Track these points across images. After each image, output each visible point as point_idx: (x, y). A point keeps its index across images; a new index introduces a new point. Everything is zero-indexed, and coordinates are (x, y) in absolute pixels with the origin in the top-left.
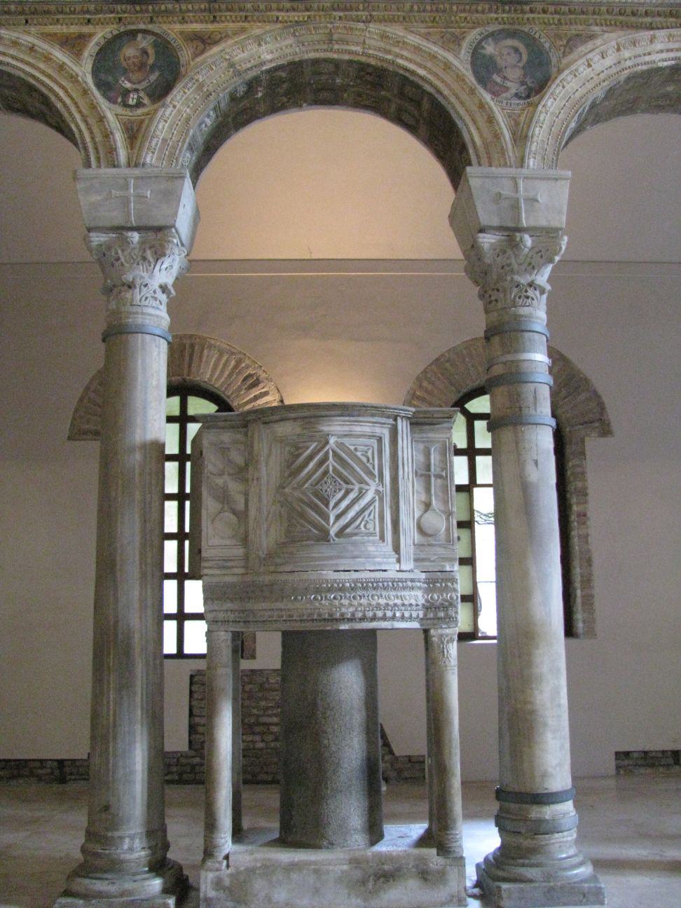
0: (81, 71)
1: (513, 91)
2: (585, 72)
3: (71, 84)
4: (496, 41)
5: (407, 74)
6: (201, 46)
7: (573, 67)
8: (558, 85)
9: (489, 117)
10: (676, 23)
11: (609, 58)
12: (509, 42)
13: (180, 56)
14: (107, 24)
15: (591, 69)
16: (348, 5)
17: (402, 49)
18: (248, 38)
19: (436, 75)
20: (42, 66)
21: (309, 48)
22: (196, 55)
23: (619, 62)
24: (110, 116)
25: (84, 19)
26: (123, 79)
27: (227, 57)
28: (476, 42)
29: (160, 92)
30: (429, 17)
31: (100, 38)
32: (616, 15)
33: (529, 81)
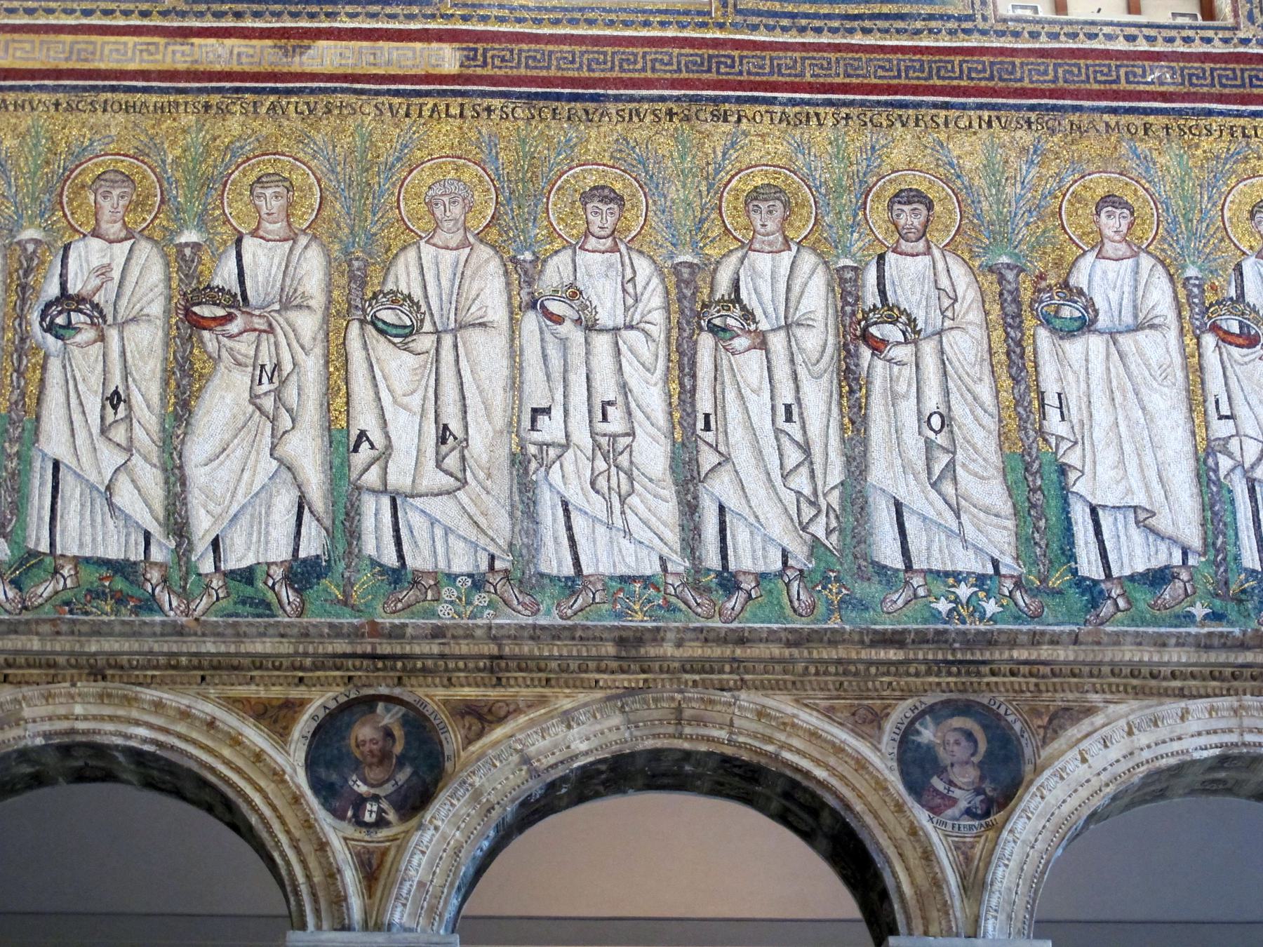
0: (288, 761)
1: (963, 805)
2: (1078, 771)
3: (273, 785)
4: (938, 721)
5: (798, 777)
6: (476, 727)
7: (1058, 765)
8: (1034, 795)
9: (925, 852)
10: (1221, 689)
11: (1116, 746)
12: (958, 722)
13: (444, 743)
14: (330, 685)
15: (1086, 765)
16: (707, 665)
17: (789, 735)
18: (549, 716)
19: (842, 778)
20: (227, 752)
21: (647, 732)
22: (469, 741)
23: (1131, 754)
24: (336, 843)
25: (294, 677)
26: (354, 778)
27: (519, 747)
28: (906, 722)
29: (414, 802)
30: (834, 682)
31: (317, 709)
32: (1126, 677)
33: (988, 787)
